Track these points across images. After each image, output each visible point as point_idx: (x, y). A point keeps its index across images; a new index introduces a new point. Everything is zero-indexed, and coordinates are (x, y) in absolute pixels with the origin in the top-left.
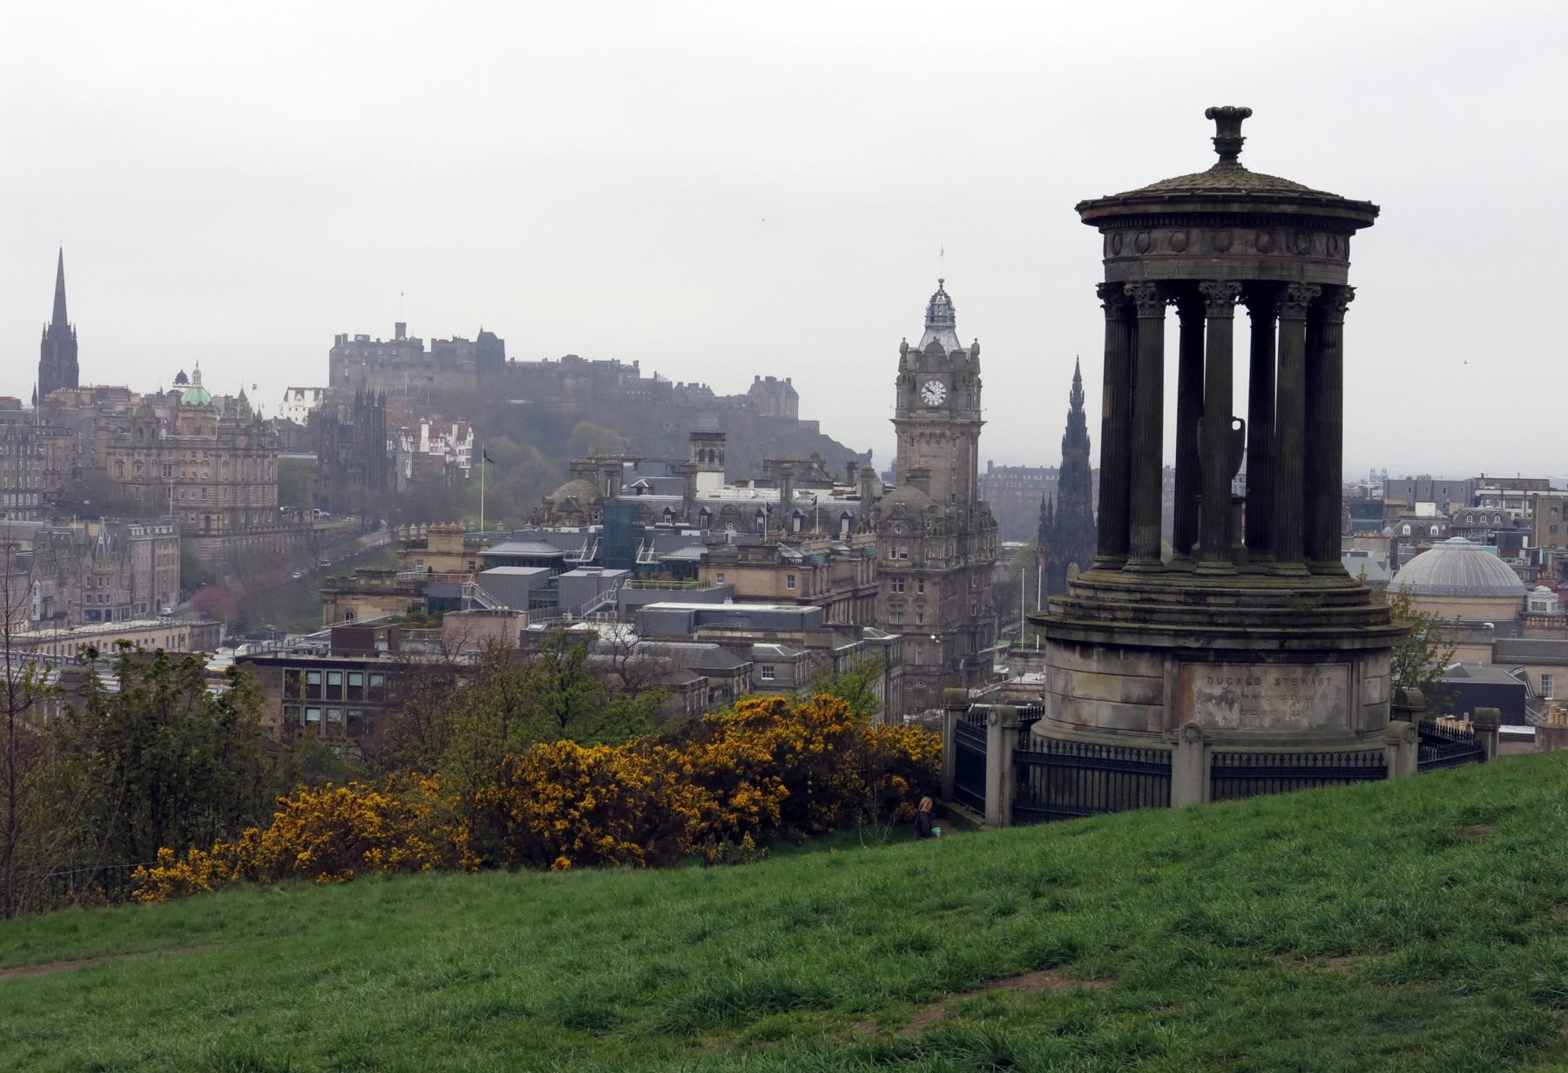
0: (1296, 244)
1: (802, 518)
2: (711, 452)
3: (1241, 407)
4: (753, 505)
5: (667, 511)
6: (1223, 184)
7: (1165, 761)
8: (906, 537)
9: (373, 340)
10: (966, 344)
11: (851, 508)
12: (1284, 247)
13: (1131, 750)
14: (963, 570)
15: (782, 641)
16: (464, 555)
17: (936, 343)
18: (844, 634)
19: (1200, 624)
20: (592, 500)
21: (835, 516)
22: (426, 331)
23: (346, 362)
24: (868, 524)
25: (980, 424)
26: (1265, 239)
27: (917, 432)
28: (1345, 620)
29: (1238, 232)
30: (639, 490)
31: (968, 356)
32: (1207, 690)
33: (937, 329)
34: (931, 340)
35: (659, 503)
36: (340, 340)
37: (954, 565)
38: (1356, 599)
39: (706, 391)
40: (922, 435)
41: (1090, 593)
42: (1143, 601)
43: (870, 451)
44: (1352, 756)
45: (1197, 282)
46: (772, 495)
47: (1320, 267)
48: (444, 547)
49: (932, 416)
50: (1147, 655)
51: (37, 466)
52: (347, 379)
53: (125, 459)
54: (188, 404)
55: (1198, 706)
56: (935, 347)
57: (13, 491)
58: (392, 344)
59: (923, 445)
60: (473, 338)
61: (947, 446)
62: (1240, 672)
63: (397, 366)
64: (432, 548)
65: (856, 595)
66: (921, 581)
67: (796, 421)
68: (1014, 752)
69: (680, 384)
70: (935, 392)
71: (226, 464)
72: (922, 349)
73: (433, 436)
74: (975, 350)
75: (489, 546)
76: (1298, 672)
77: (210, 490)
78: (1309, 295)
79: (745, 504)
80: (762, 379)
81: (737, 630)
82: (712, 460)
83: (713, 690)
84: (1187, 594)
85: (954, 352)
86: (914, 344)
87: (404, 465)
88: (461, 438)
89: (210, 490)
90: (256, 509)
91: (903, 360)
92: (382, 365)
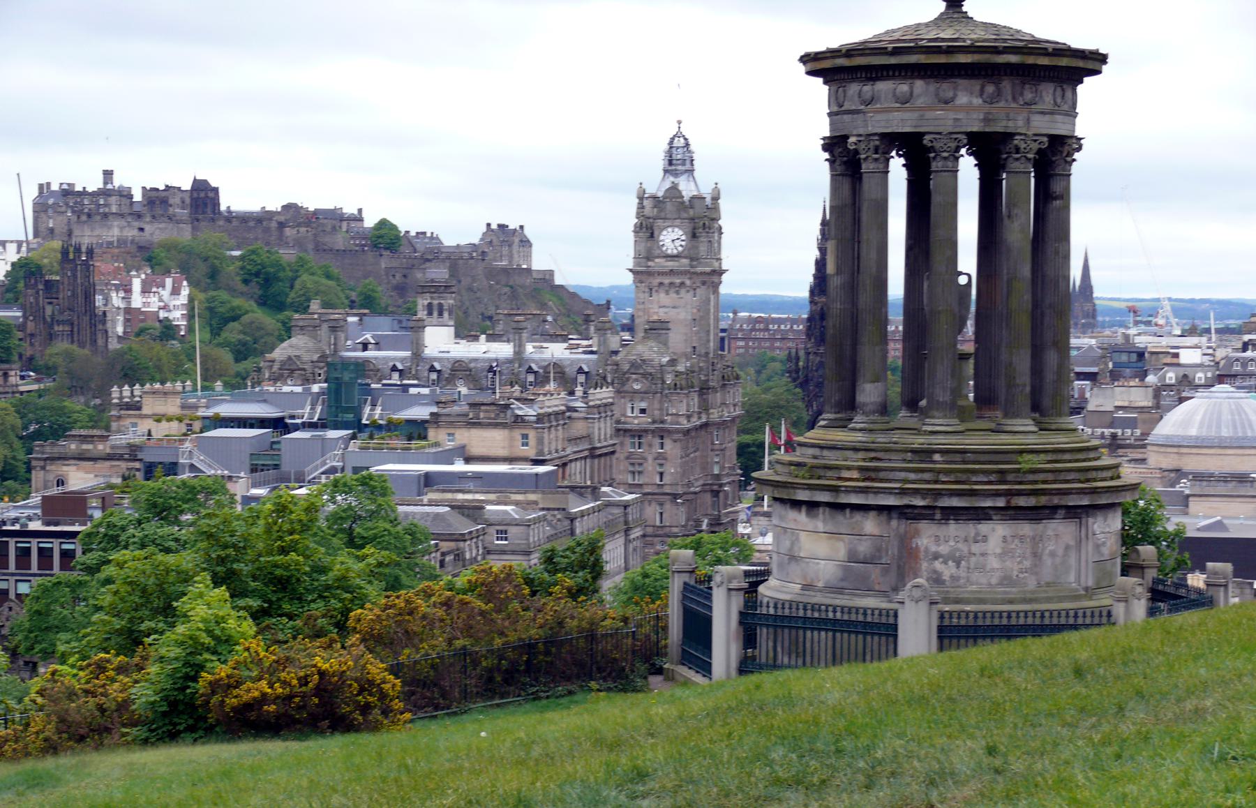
0: (1022, 94)
2: (440, 305)
3: (896, 286)
4: (484, 360)
5: (394, 369)
6: (947, 34)
7: (891, 621)
8: (645, 393)
9: (78, 188)
10: (706, 190)
11: (587, 362)
12: (1010, 98)
13: (857, 609)
14: (705, 426)
15: (517, 503)
17: (674, 187)
18: (581, 495)
19: (928, 482)
20: (315, 357)
21: (570, 371)
23: (50, 211)
24: (604, 378)
25: (720, 272)
26: (990, 89)
28: (1071, 476)
29: (962, 83)
30: (365, 346)
31: (708, 201)
32: (933, 548)
33: (676, 174)
34: (667, 185)
35: (386, 359)
37: (696, 422)
38: (1092, 455)
39: (433, 238)
40: (661, 284)
41: (816, 451)
42: (872, 459)
43: (608, 302)
44: (1080, 614)
45: (922, 135)
46: (504, 350)
47: (1047, 117)
49: (671, 264)
50: (872, 514)
52: (52, 231)
55: (924, 565)
59: (662, 295)
60: (187, 186)
61: (687, 296)
62: (970, 529)
63: (105, 216)
65: (593, 454)
66: (662, 437)
67: (529, 270)
68: (741, 613)
69: (407, 232)
70: (672, 239)
72: (660, 194)
73: (145, 291)
75: (207, 407)
76: (1026, 528)
78: (1035, 146)
79: (475, 360)
80: (494, 226)
81: (469, 492)
83: (443, 554)
84: (914, 451)
85: (693, 198)
87: (114, 322)
88: (176, 292)
91: (641, 207)
92: (89, 216)
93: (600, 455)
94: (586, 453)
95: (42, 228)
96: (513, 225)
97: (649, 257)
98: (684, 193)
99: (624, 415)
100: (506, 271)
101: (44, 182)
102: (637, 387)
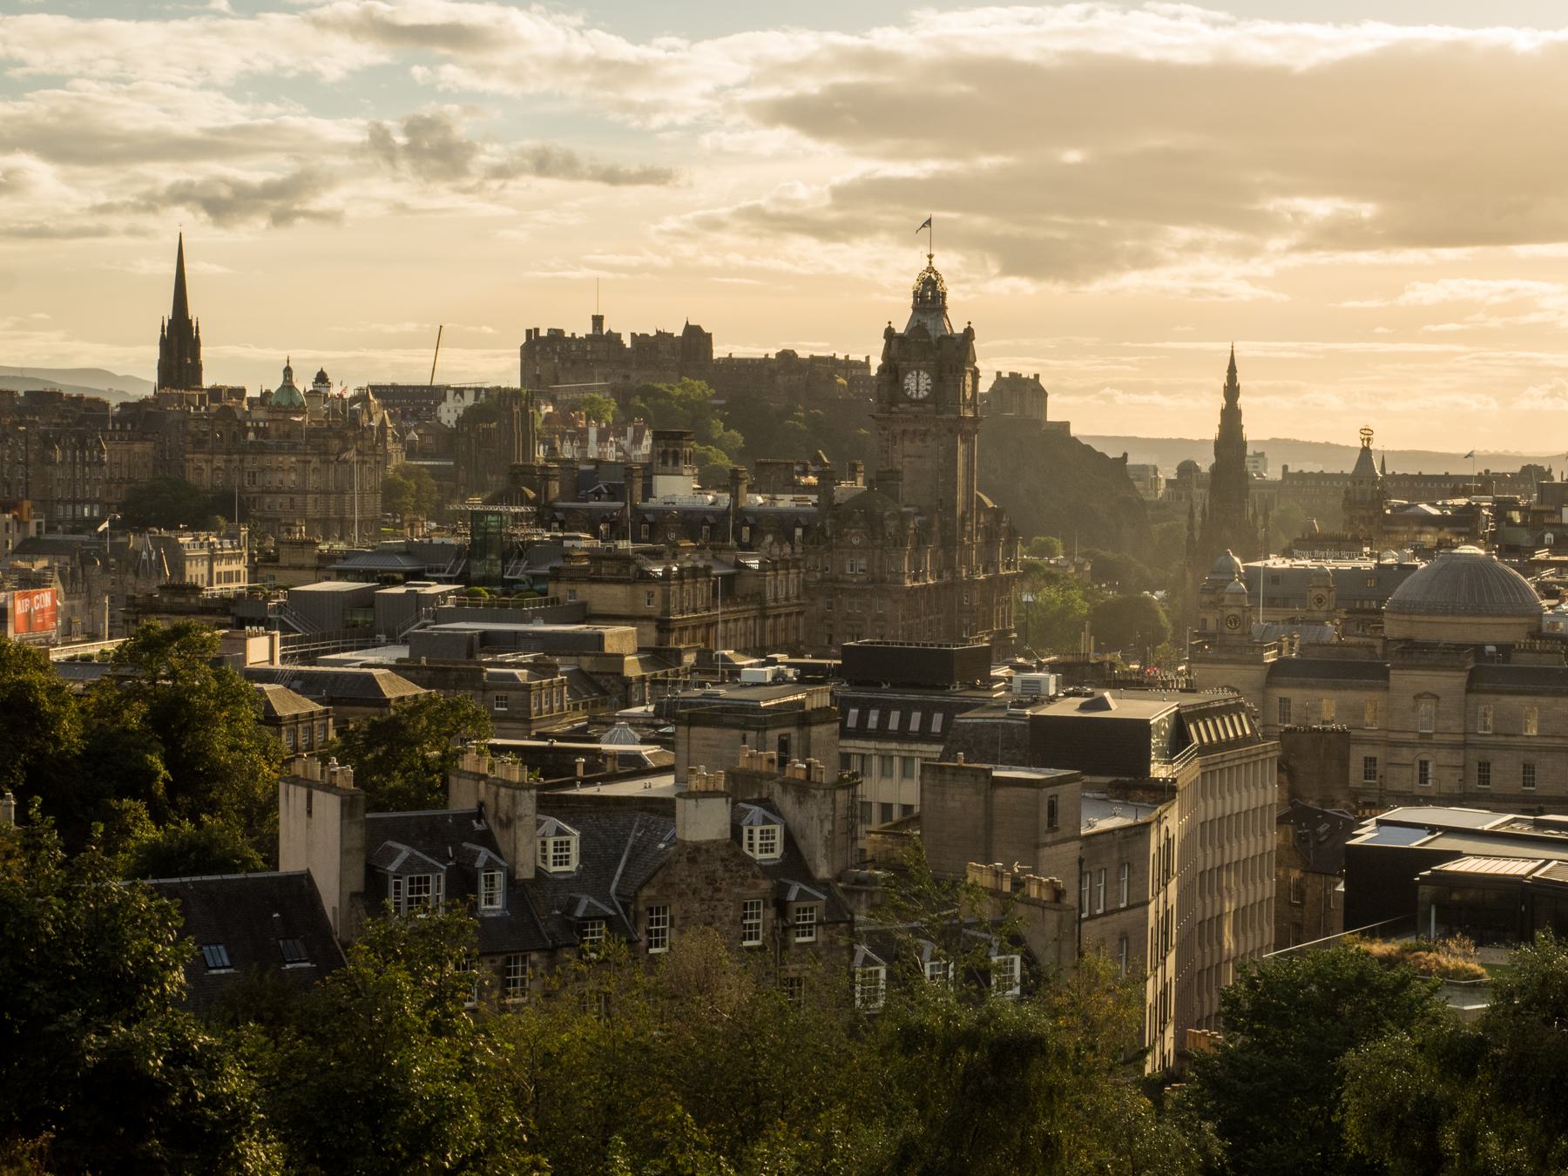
1: (752, 527)
9: (568, 335)
10: (959, 329)
22: (626, 324)
24: (824, 533)
40: (904, 432)
43: (1125, 455)
48: (297, 560)
54: (278, 404)
57: (67, 502)
59: (907, 443)
60: (678, 333)
64: (283, 561)
73: (602, 438)
74: (969, 333)
77: (298, 499)
86: (900, 328)
89: (298, 499)
91: (888, 347)
92: (574, 363)
93: (777, 616)
94: (754, 613)
96: (1027, 372)
97: (893, 402)
98: (932, 333)
99: (843, 573)
101: (531, 327)
102: (855, 541)
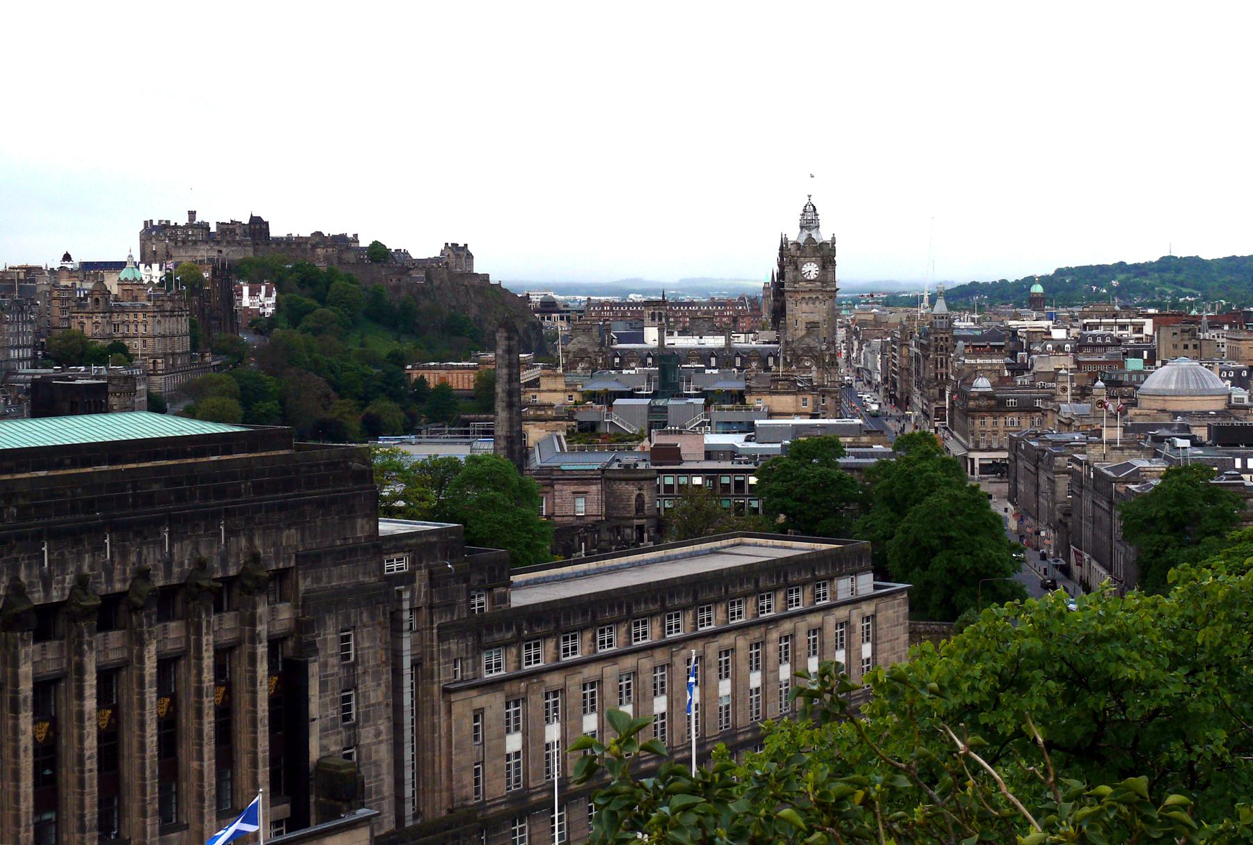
9: (172, 224)
16: (565, 391)
22: (212, 216)
27: (800, 297)
33: (809, 229)
36: (148, 225)
39: (406, 253)
48: (552, 387)
51: (29, 328)
52: (155, 252)
53: (85, 321)
56: (810, 239)
58: (187, 226)
60: (246, 221)
71: (159, 322)
73: (252, 294)
82: (660, 319)
88: (268, 295)
89: (149, 341)
90: (179, 354)
92: (184, 243)
95: (148, 251)
100: (462, 275)
